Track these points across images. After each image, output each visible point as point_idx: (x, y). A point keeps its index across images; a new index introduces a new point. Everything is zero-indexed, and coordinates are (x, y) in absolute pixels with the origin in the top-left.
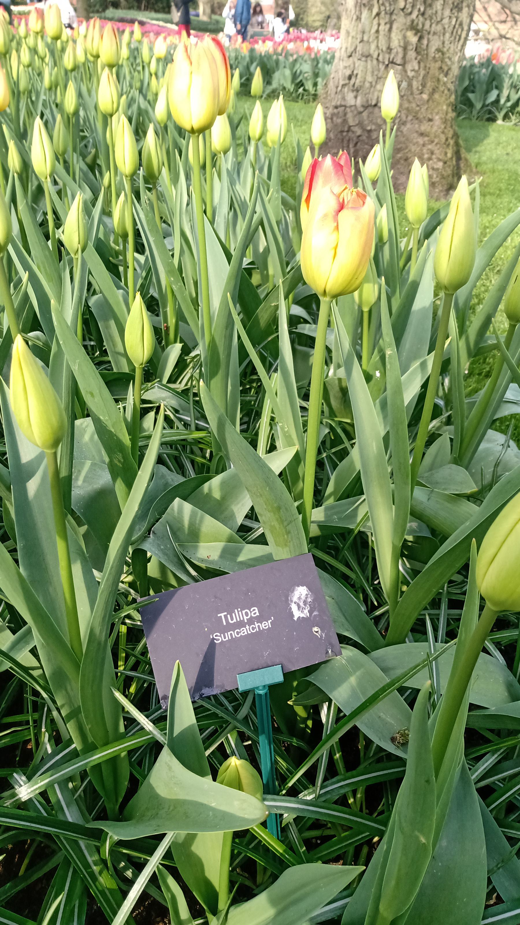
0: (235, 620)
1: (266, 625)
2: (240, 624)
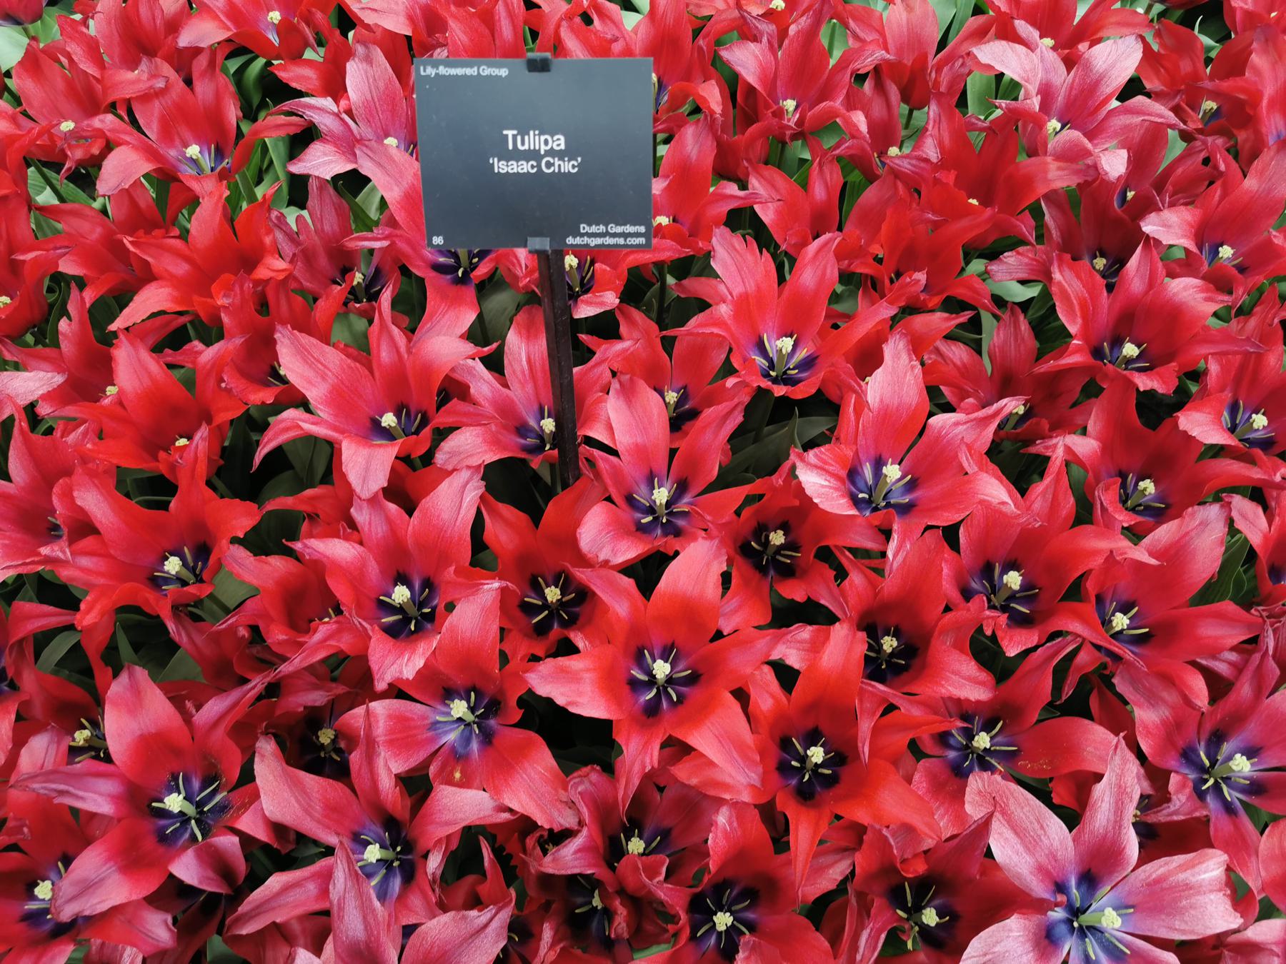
0: (526, 147)
1: (568, 167)
2: (533, 155)
